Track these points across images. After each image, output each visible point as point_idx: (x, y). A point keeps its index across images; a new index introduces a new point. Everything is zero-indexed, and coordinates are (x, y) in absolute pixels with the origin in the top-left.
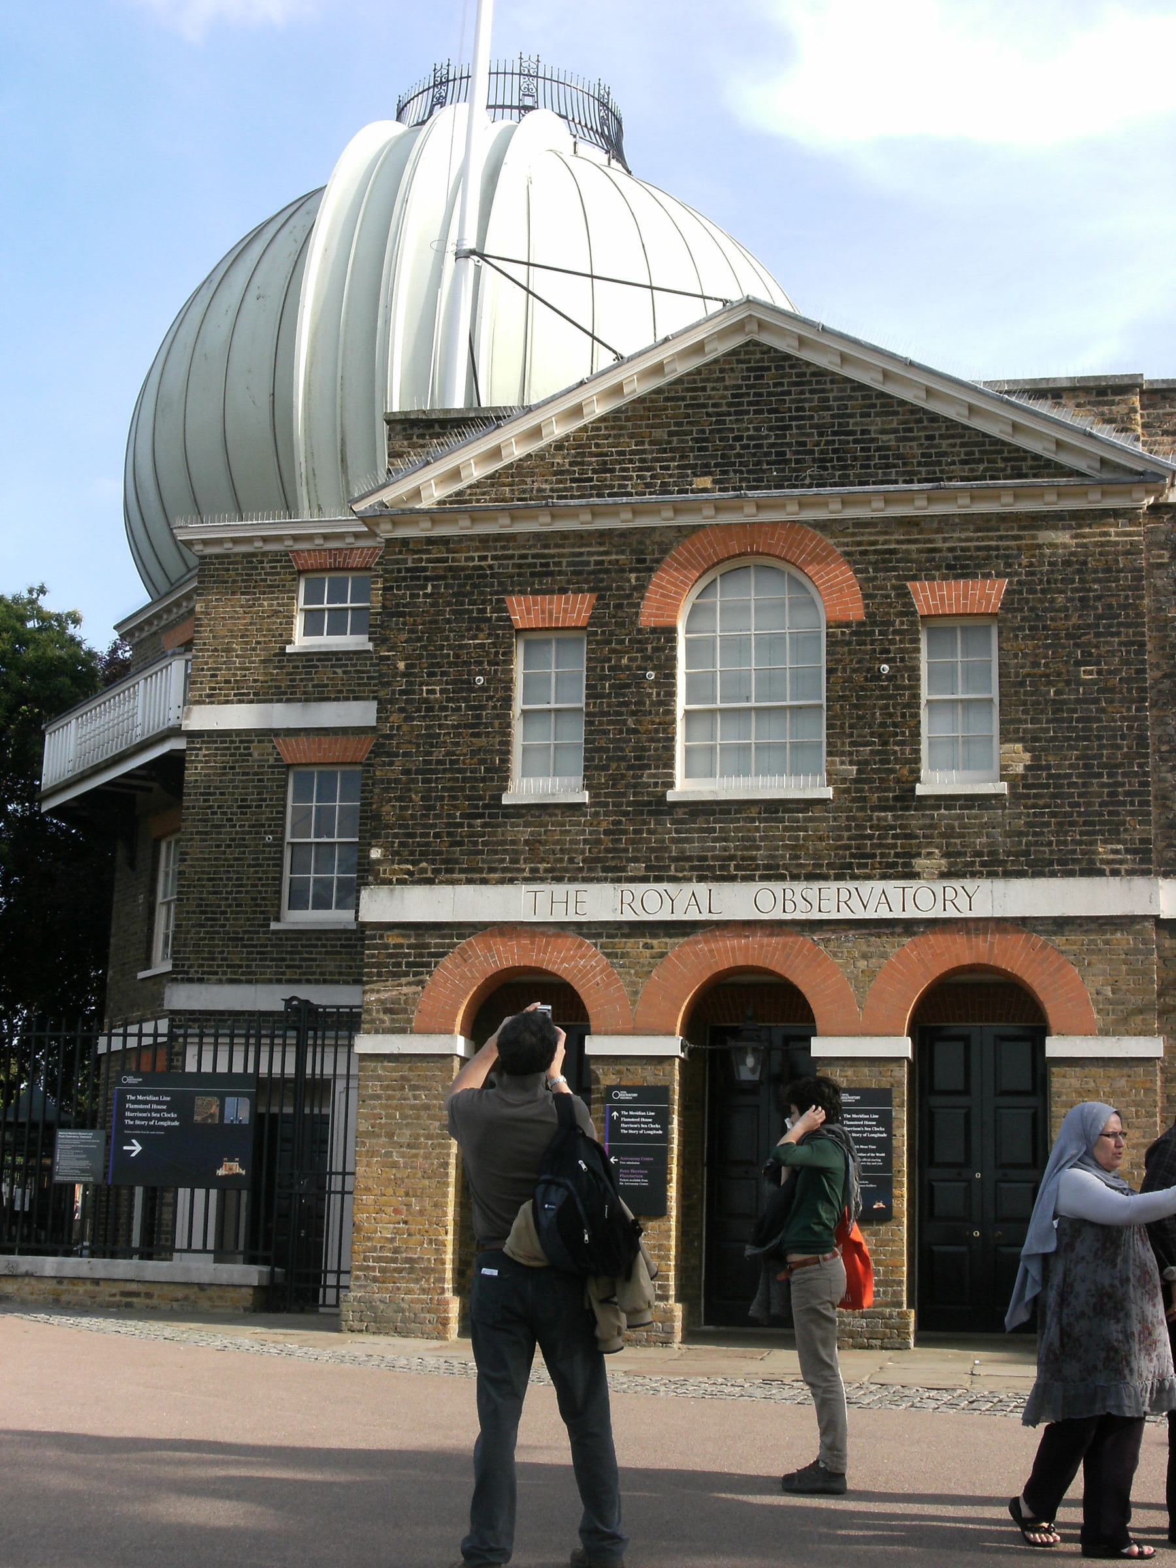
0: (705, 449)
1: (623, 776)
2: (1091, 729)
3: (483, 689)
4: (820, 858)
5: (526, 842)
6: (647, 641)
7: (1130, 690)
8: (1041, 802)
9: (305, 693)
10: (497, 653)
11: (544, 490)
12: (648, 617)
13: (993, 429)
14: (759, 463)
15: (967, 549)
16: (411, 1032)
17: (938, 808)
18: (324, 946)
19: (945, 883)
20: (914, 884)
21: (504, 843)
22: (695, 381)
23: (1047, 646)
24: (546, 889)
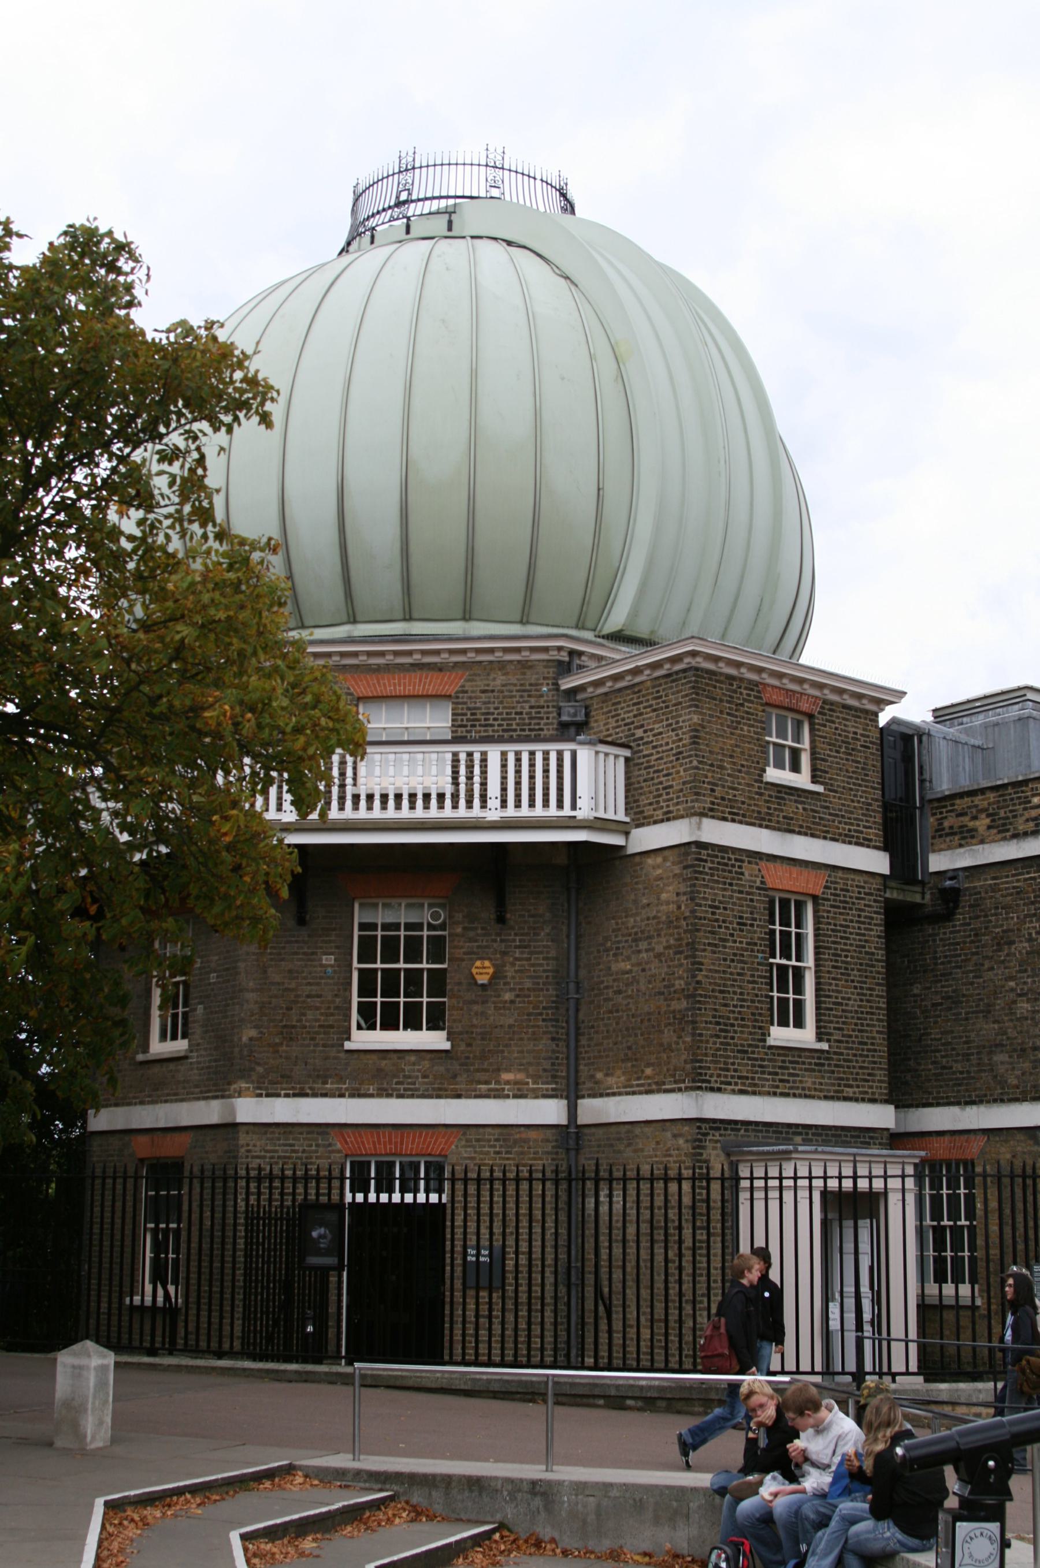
9: (778, 822)
18: (804, 1063)
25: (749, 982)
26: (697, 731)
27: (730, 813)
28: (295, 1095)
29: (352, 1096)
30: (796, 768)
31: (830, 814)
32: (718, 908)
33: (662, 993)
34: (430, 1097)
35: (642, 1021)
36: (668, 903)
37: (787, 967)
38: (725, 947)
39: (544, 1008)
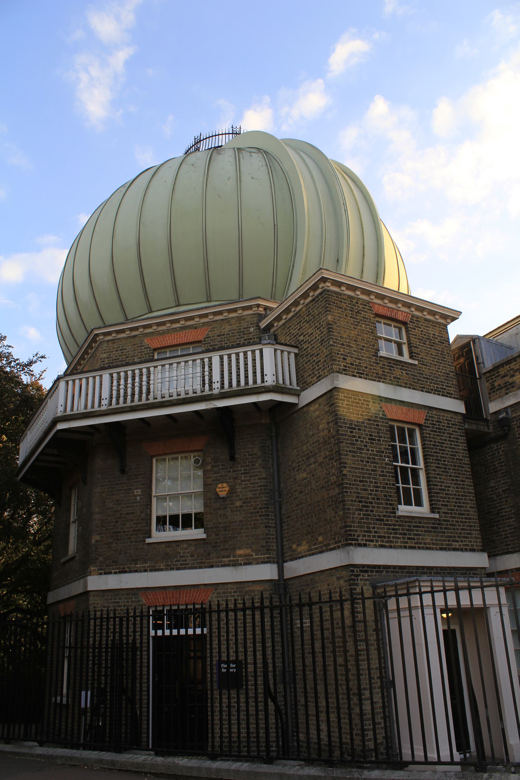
18: (423, 527)
25: (380, 475)
26: (331, 324)
27: (357, 373)
28: (120, 572)
29: (151, 571)
30: (401, 353)
31: (424, 378)
32: (355, 429)
33: (324, 487)
34: (195, 568)
35: (315, 507)
36: (323, 430)
37: (407, 468)
38: (361, 453)
39: (260, 508)
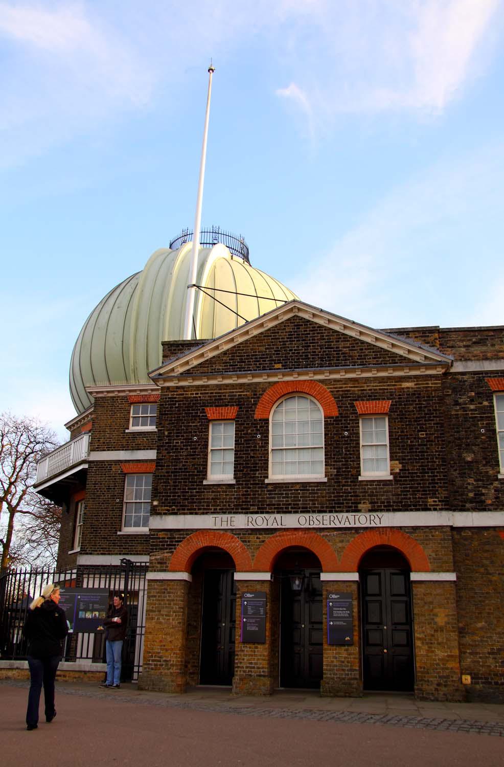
0: (279, 354)
1: (249, 474)
2: (424, 455)
3: (196, 442)
4: (323, 504)
5: (212, 499)
6: (257, 424)
7: (438, 441)
8: (406, 483)
10: (202, 428)
11: (220, 369)
12: (258, 415)
13: (384, 346)
14: (299, 359)
15: (376, 390)
16: (168, 571)
17: (367, 485)
18: (137, 541)
19: (370, 514)
20: (359, 514)
21: (204, 499)
22: (274, 330)
23: (407, 425)
24: (219, 517)
